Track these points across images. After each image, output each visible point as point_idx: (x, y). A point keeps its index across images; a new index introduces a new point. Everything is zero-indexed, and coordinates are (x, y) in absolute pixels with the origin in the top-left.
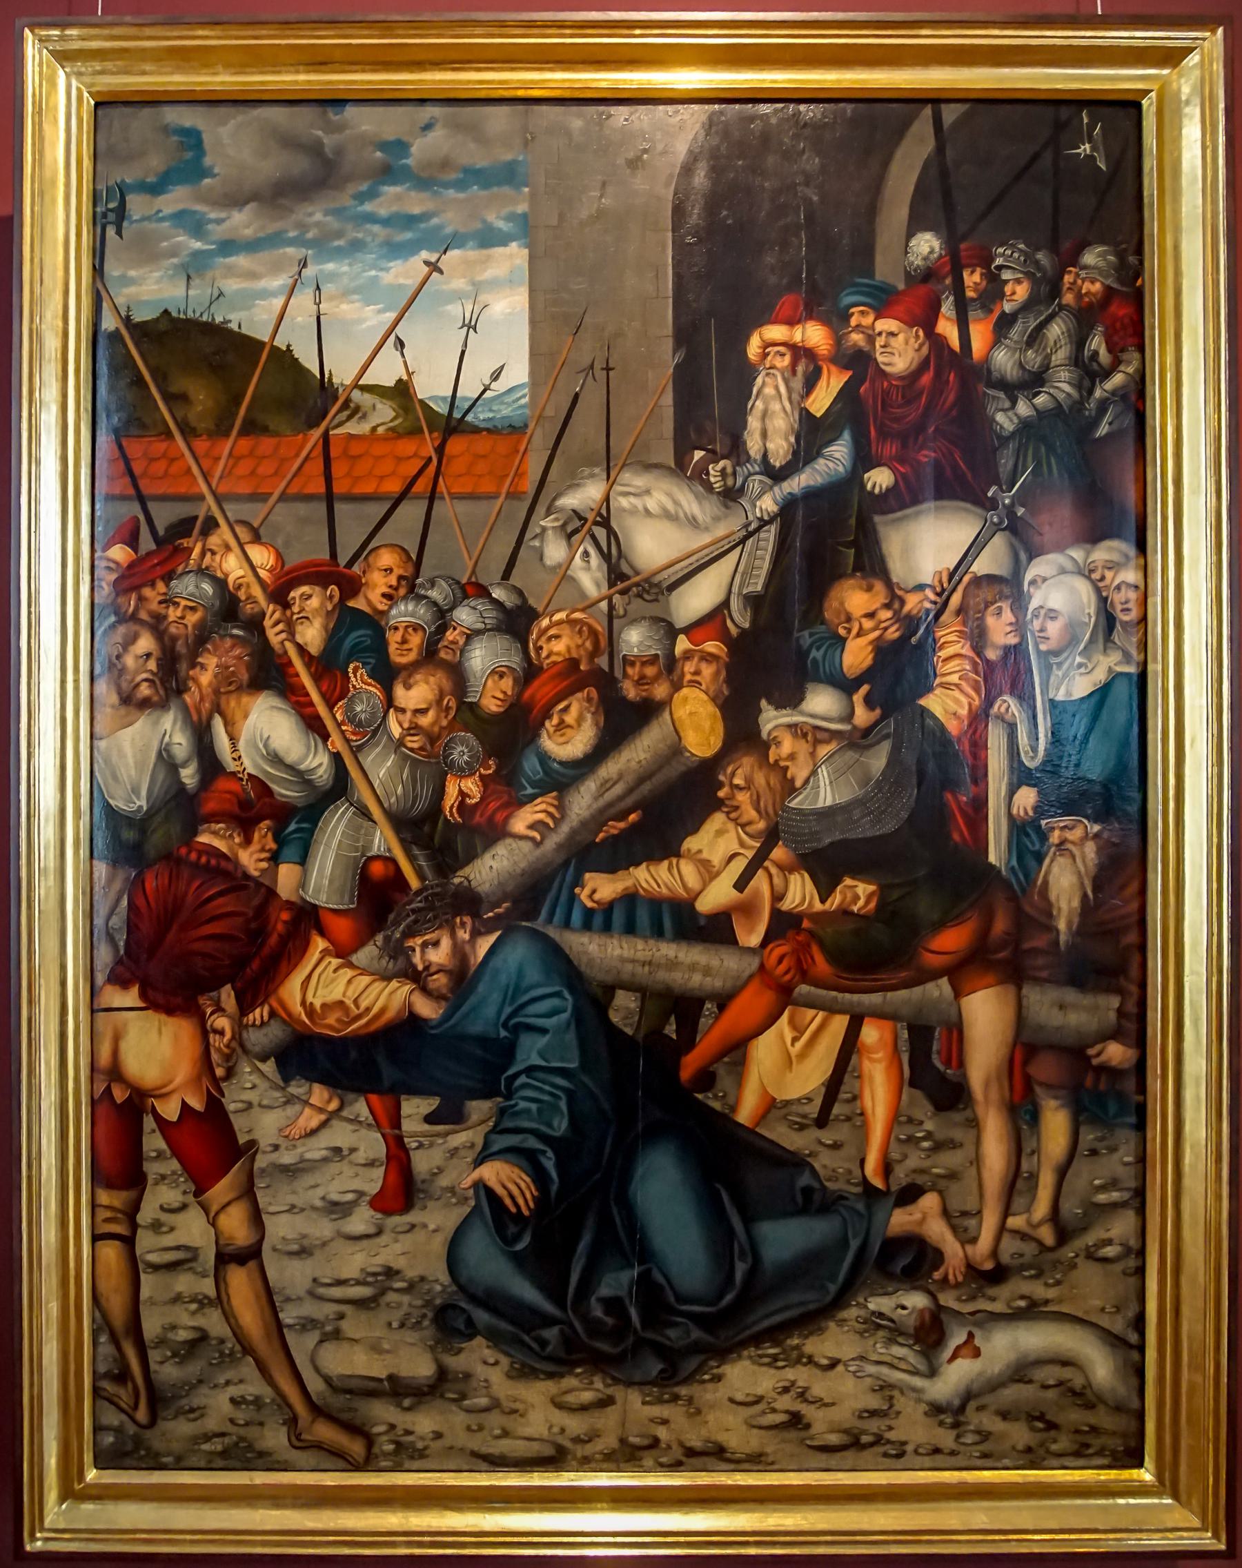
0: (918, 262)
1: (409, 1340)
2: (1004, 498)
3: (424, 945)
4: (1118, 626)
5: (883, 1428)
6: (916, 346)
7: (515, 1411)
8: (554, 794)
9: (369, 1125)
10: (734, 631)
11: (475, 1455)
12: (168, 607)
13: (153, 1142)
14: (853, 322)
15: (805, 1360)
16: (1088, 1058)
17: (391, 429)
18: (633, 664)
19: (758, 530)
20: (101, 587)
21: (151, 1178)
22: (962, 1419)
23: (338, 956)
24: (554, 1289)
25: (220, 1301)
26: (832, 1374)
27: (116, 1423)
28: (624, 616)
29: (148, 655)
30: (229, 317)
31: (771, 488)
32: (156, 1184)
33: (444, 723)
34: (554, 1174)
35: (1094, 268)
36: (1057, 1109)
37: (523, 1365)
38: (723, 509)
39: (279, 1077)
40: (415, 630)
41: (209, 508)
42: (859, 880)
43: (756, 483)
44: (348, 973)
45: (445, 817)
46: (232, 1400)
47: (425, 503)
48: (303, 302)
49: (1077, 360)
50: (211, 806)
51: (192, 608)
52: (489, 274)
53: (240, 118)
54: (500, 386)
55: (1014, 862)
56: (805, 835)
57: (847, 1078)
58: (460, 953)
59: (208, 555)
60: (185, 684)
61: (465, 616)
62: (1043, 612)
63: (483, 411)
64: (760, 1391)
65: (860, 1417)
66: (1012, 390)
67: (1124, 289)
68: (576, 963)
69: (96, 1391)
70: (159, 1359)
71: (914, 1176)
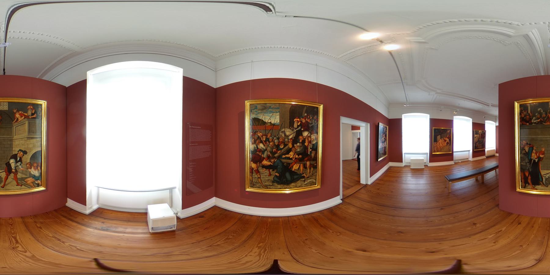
49: (314, 122)
58: (274, 161)
61: (275, 138)
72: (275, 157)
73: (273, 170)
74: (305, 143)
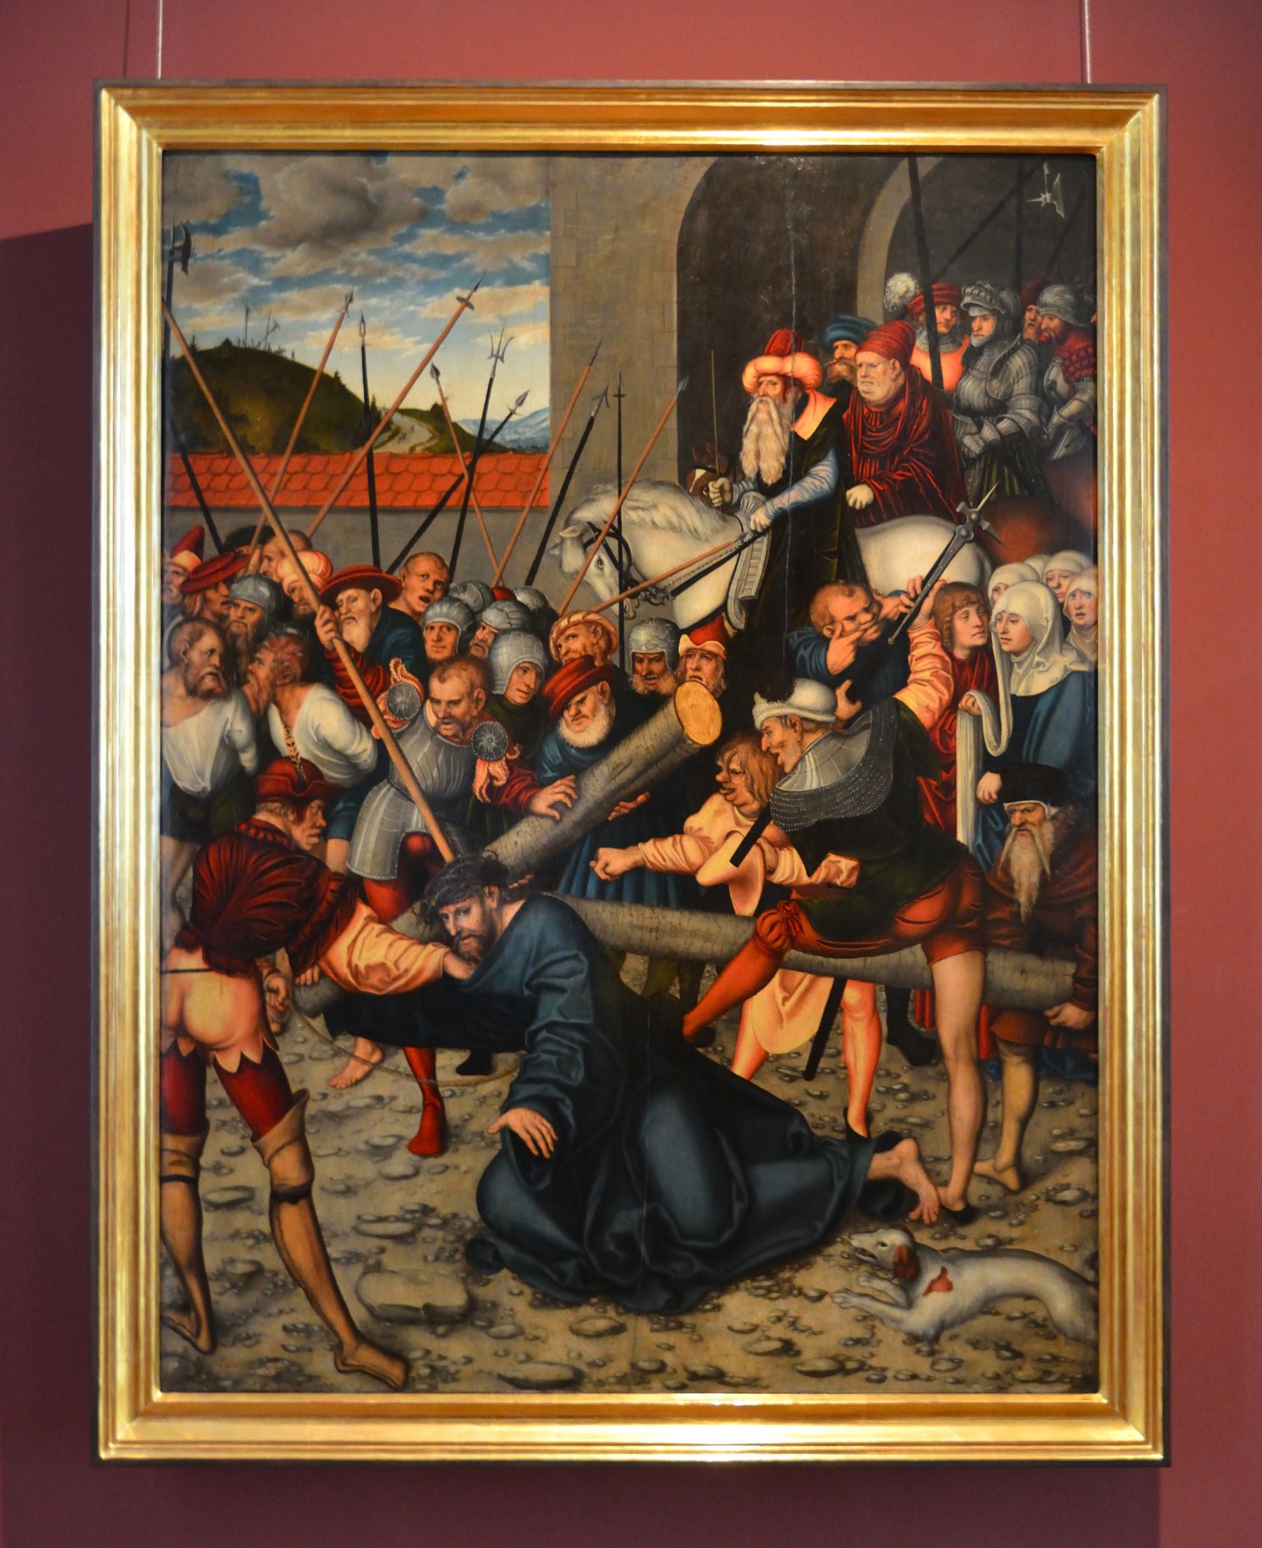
0: (896, 300)
1: (442, 1272)
2: (970, 515)
3: (457, 912)
4: (1073, 629)
5: (866, 1355)
6: (894, 376)
7: (536, 1338)
8: (572, 777)
9: (407, 1075)
10: (731, 632)
11: (502, 1378)
12: (229, 608)
13: (215, 1091)
14: (837, 354)
15: (795, 1292)
16: (1047, 1019)
17: (429, 449)
18: (641, 661)
19: (752, 541)
20: (171, 590)
21: (213, 1124)
22: (936, 1347)
23: (380, 922)
24: (572, 1226)
25: (274, 1236)
26: (820, 1305)
27: (180, 1350)
28: (634, 617)
29: (212, 651)
30: (283, 347)
31: (764, 503)
32: (218, 1129)
33: (475, 713)
34: (571, 1120)
35: (1054, 305)
36: (1018, 1064)
37: (545, 1295)
38: (721, 522)
39: (326, 1030)
40: (449, 629)
41: (266, 519)
42: (841, 855)
43: (751, 498)
44: (388, 938)
45: (475, 797)
46: (285, 1329)
47: (457, 517)
48: (350, 332)
50: (268, 787)
51: (251, 610)
52: (515, 309)
53: (293, 166)
54: (524, 411)
55: (980, 841)
56: (793, 815)
57: (831, 1035)
58: (488, 919)
59: (266, 561)
60: (245, 677)
61: (493, 617)
62: (1005, 616)
63: (509, 433)
64: (756, 1320)
65: (846, 1345)
66: (978, 416)
67: (1081, 325)
68: (591, 929)
69: (162, 1320)
70: (218, 1290)
71: (891, 1124)
72: (495, 874)
73: (478, 1066)
74: (903, 684)
